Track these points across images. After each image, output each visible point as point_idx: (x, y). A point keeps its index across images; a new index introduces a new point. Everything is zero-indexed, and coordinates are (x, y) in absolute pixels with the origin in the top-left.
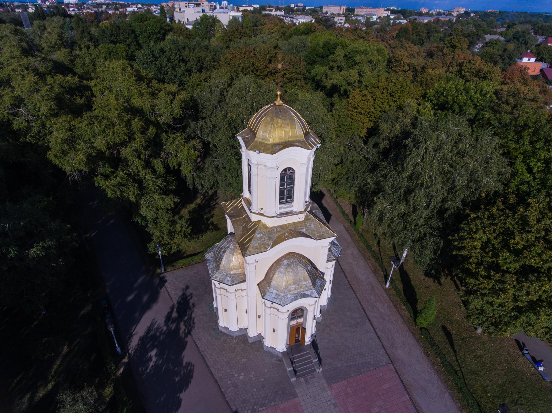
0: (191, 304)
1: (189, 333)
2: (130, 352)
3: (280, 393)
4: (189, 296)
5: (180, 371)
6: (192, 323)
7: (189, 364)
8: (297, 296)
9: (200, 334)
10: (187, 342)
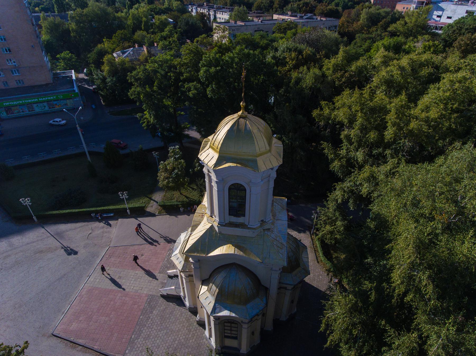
3: (168, 265)
8: (180, 241)
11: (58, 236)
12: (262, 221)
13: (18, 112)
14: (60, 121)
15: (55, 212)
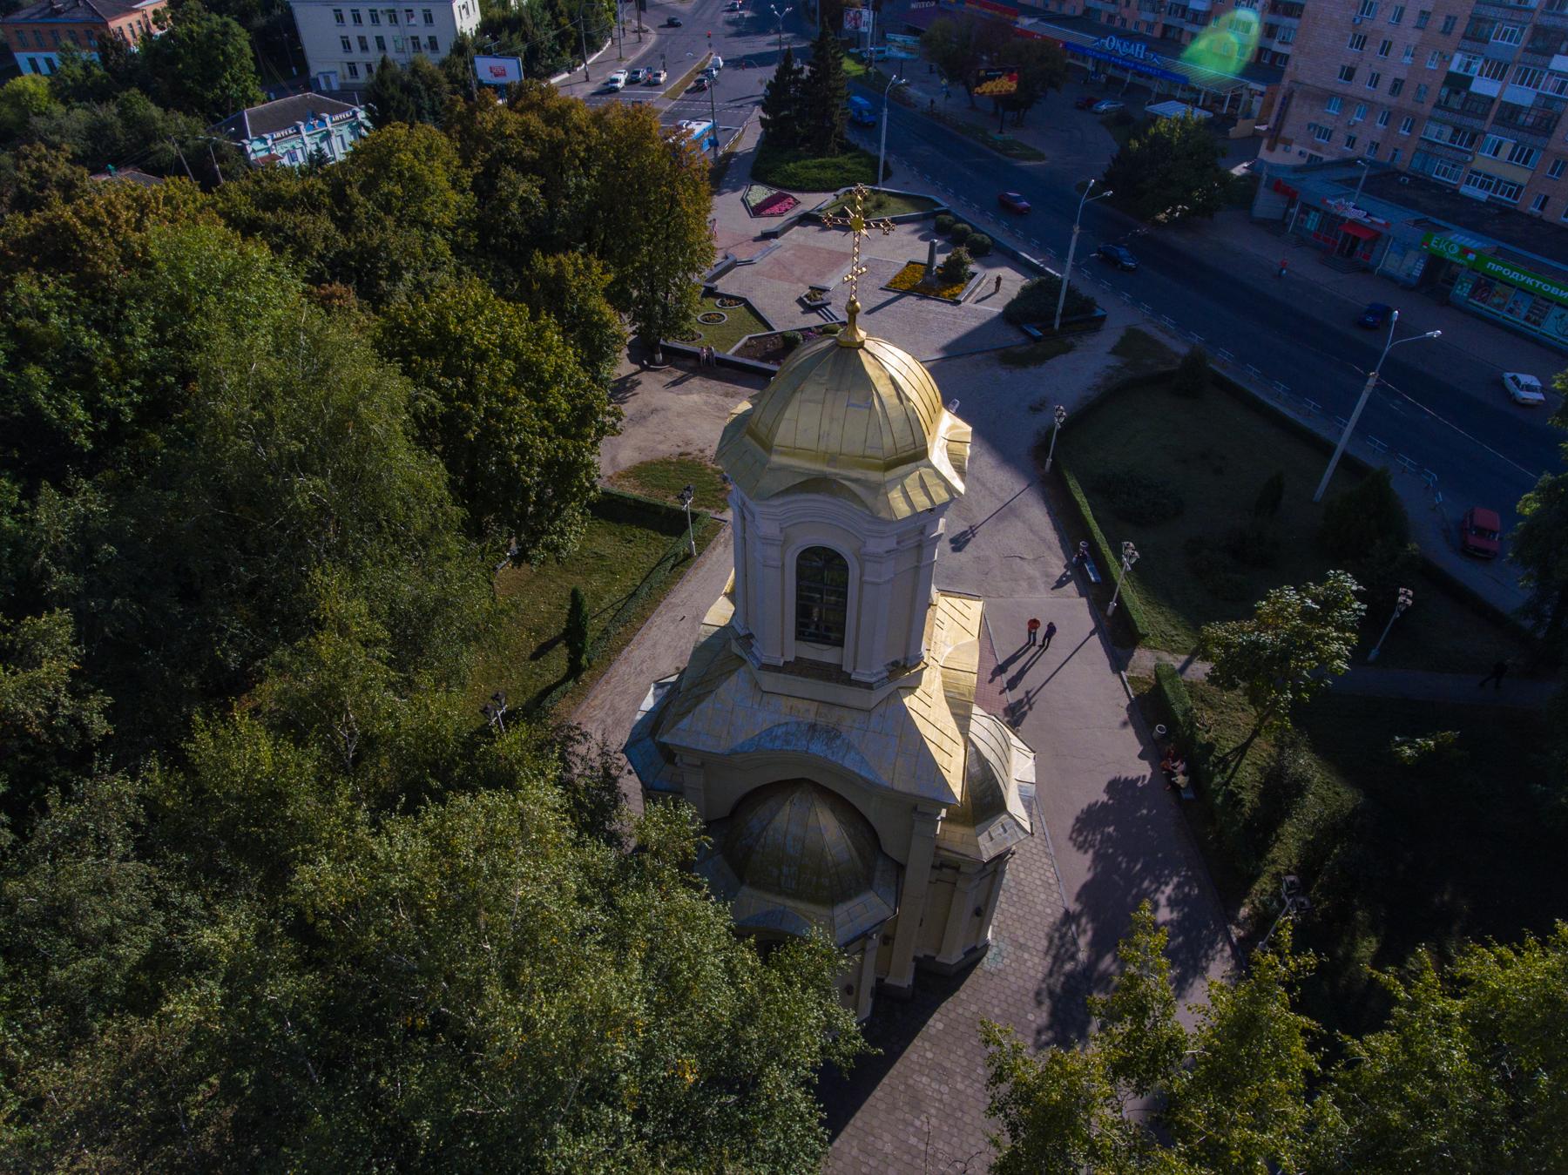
0: (1047, 1003)
1: (1069, 918)
2: (1228, 948)
4: (1047, 1044)
5: (1101, 842)
6: (1056, 941)
7: (1081, 847)
9: (1043, 896)
10: (1078, 898)
11: (1006, 512)
12: (750, 636)
13: (1498, 306)
14: (1529, 388)
15: (1073, 483)
